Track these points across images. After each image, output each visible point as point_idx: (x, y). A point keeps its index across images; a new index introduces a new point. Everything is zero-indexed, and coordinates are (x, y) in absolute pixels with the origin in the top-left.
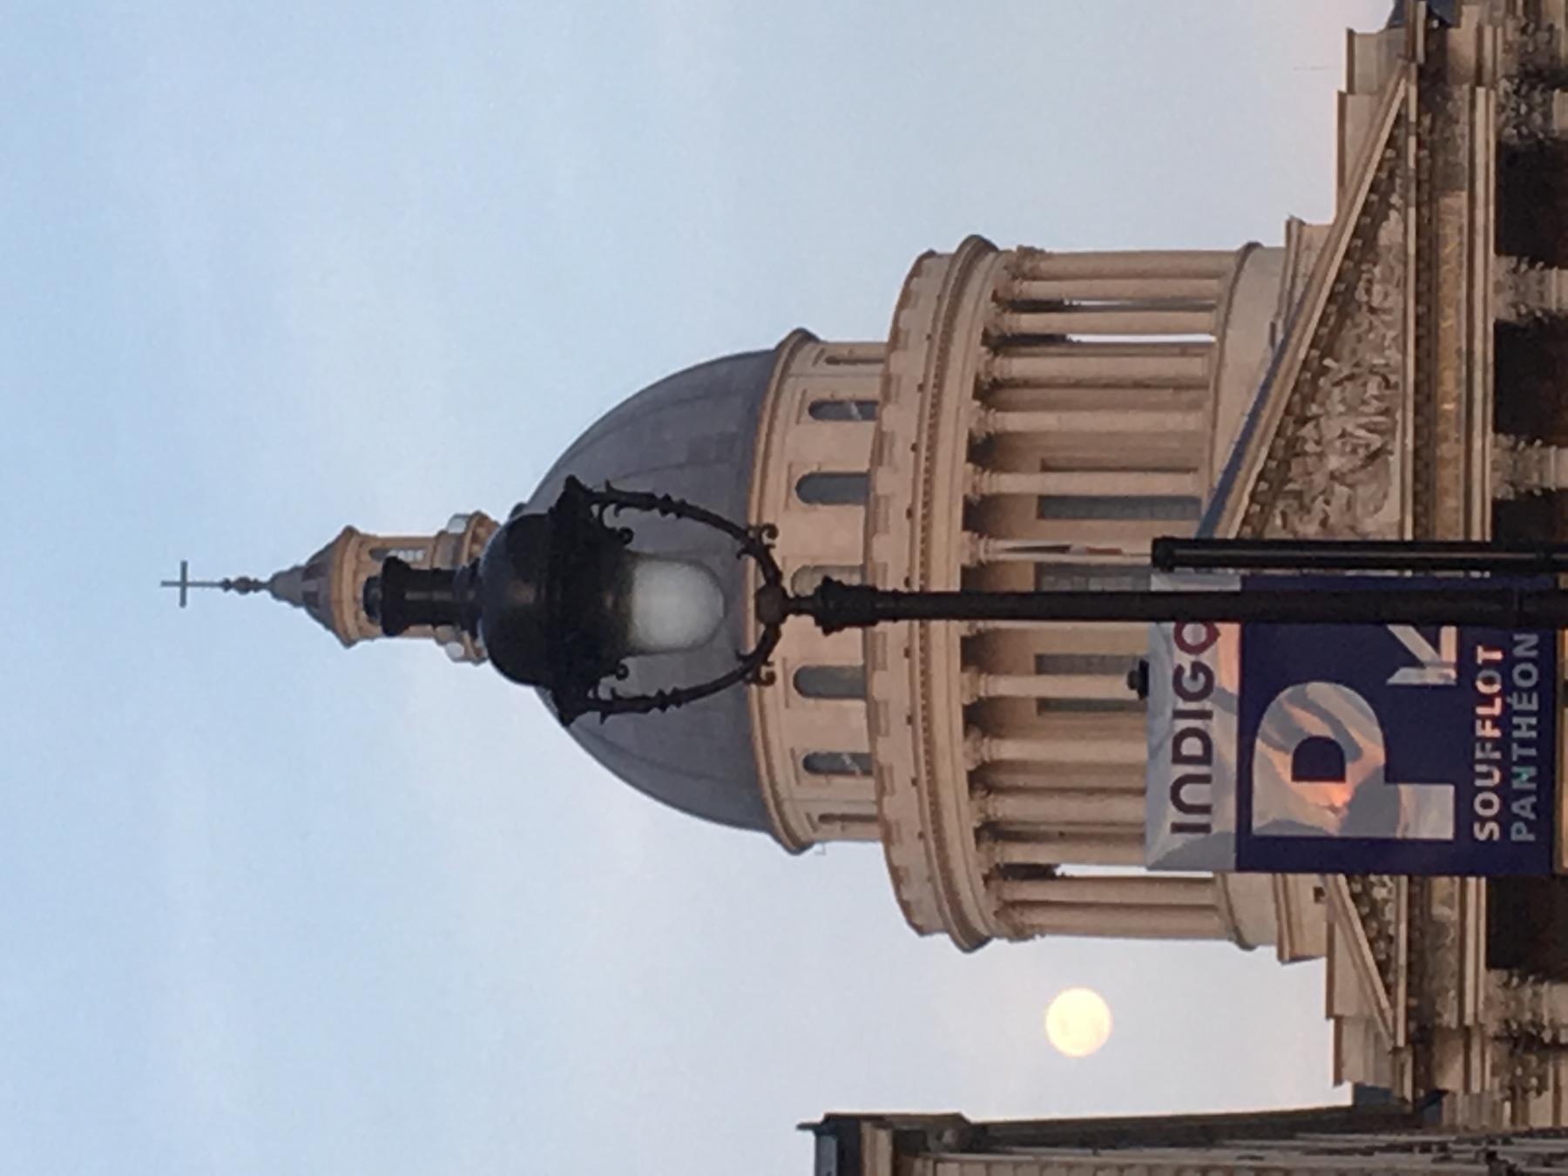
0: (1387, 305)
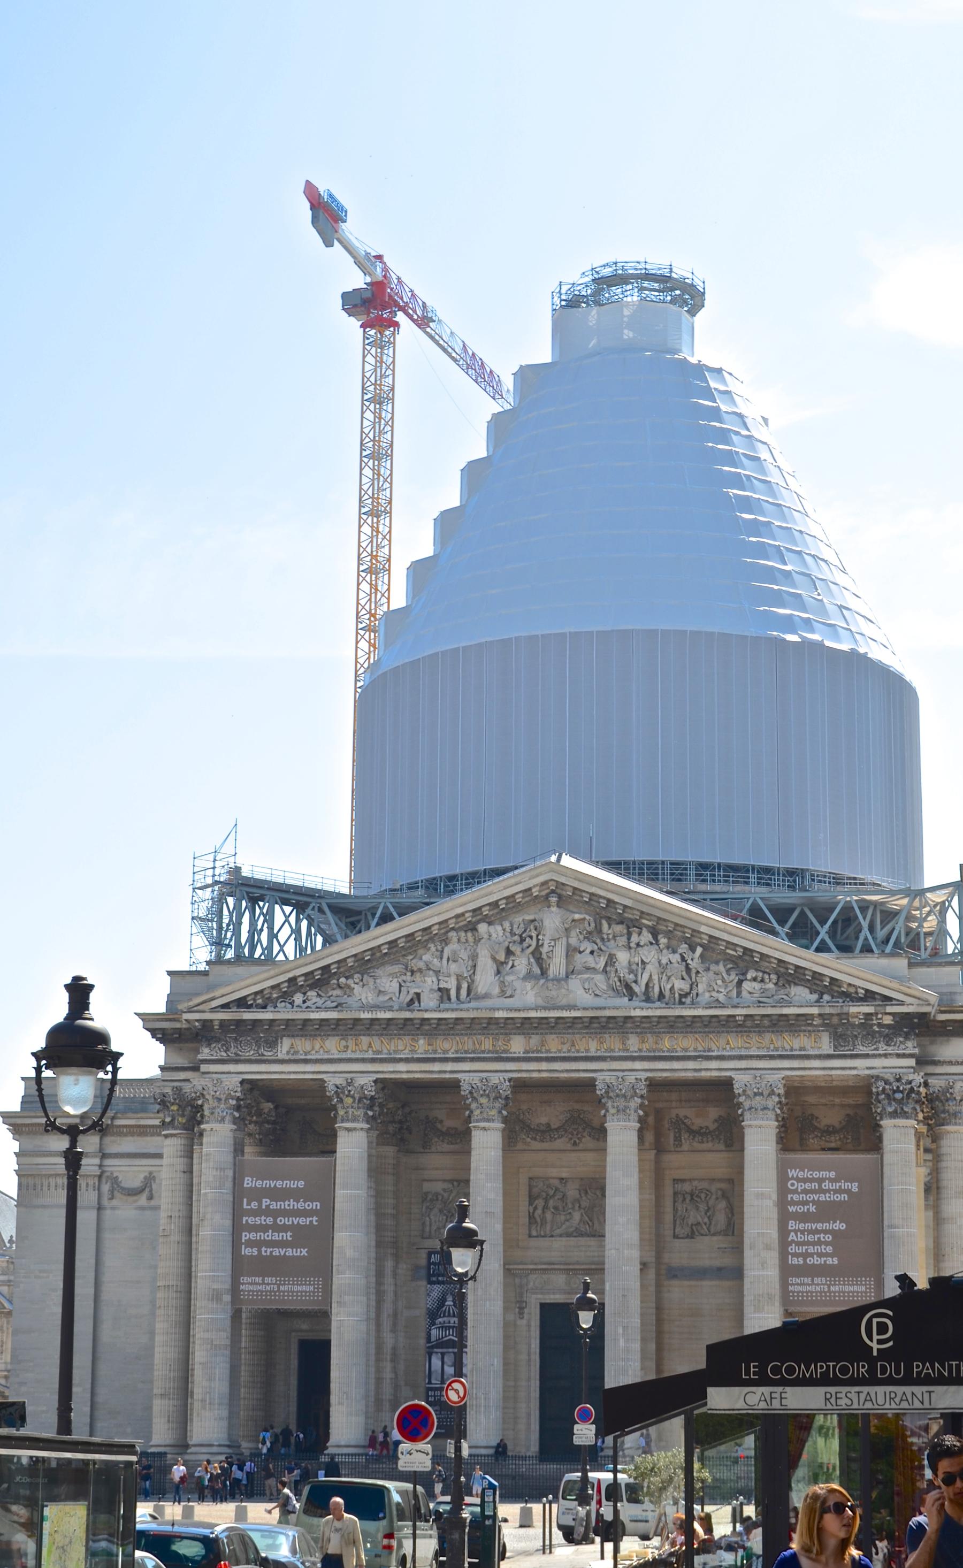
0: (744, 994)
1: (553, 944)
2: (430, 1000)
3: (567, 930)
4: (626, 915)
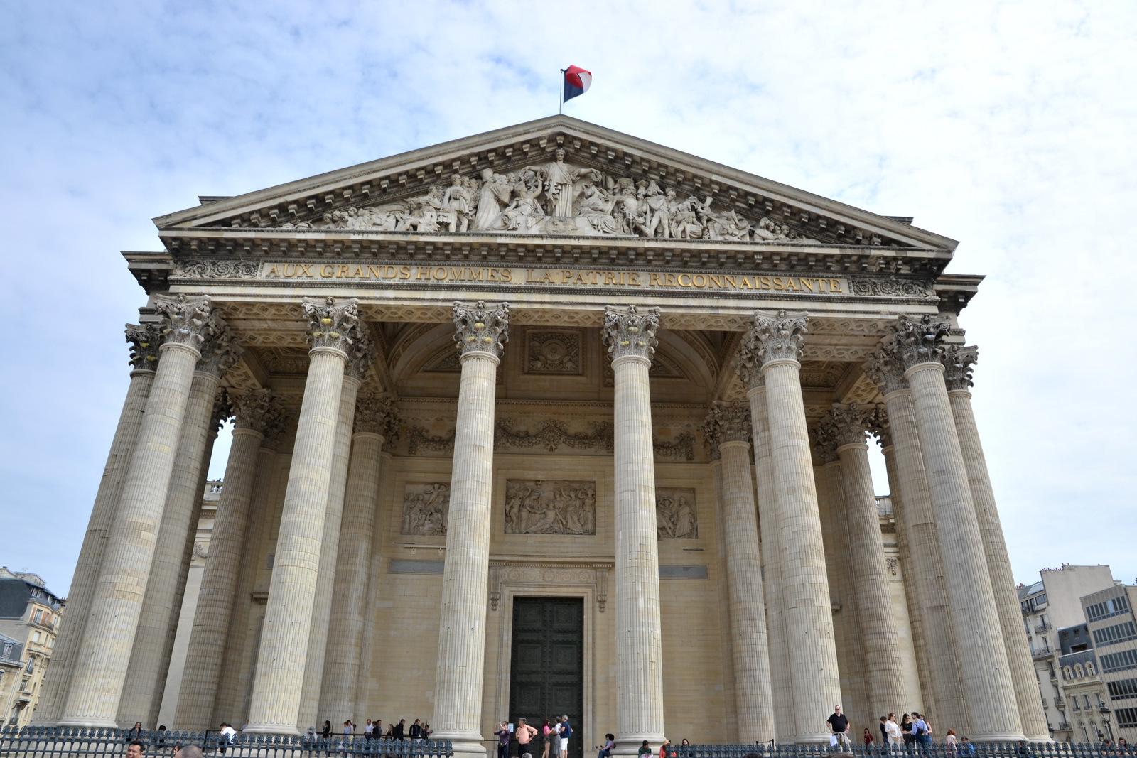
3: (574, 182)
4: (633, 170)
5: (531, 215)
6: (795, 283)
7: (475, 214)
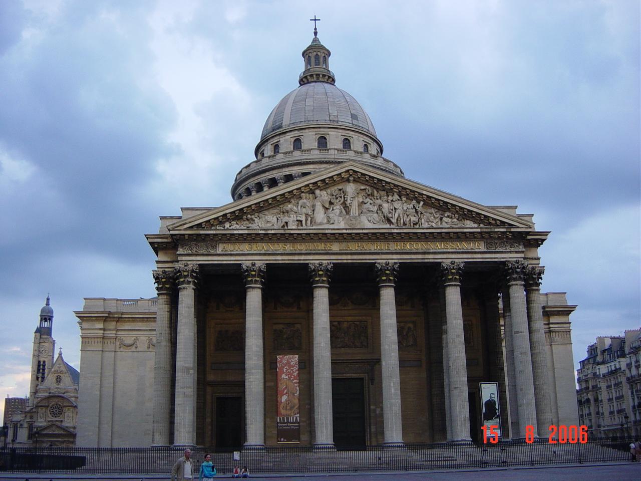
0: (444, 223)
1: (352, 199)
2: (292, 226)
3: (358, 193)
5: (341, 214)
6: (460, 245)
7: (313, 213)
